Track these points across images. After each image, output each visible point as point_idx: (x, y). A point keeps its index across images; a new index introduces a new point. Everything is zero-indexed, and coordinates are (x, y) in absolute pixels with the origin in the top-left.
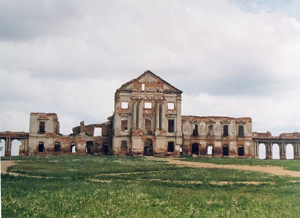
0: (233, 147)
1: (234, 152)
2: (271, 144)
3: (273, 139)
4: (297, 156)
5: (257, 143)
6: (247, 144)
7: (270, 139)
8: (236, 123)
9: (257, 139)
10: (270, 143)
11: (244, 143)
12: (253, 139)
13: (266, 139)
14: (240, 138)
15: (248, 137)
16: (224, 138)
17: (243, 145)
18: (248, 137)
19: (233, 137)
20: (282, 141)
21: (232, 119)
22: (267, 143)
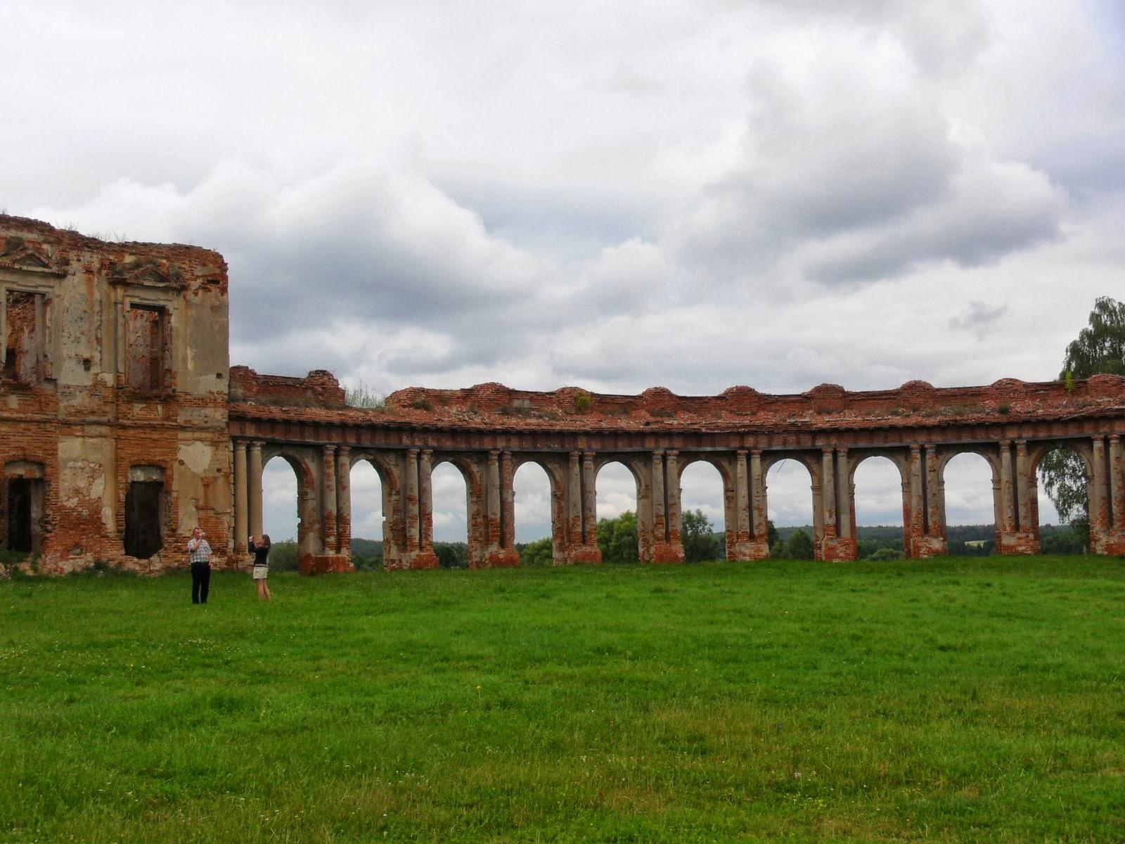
0: (82, 484)
1: (95, 521)
2: (345, 459)
3: (373, 428)
4: (503, 544)
5: (257, 451)
6: (197, 457)
7: (343, 427)
8: (114, 283)
9: (257, 421)
10: (337, 454)
11: (175, 450)
12: (237, 418)
13: (302, 421)
14: (138, 409)
15: (202, 402)
16: (14, 401)
17: (162, 469)
18: (202, 402)
19: (80, 400)
20: (407, 435)
21: (74, 241)
22: (319, 450)
